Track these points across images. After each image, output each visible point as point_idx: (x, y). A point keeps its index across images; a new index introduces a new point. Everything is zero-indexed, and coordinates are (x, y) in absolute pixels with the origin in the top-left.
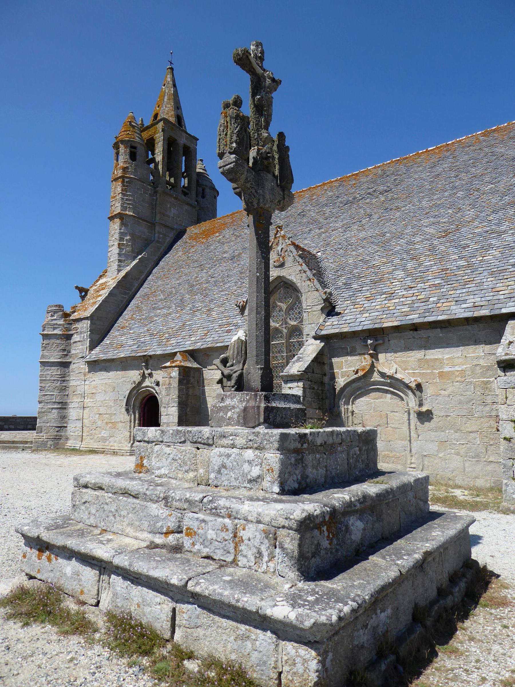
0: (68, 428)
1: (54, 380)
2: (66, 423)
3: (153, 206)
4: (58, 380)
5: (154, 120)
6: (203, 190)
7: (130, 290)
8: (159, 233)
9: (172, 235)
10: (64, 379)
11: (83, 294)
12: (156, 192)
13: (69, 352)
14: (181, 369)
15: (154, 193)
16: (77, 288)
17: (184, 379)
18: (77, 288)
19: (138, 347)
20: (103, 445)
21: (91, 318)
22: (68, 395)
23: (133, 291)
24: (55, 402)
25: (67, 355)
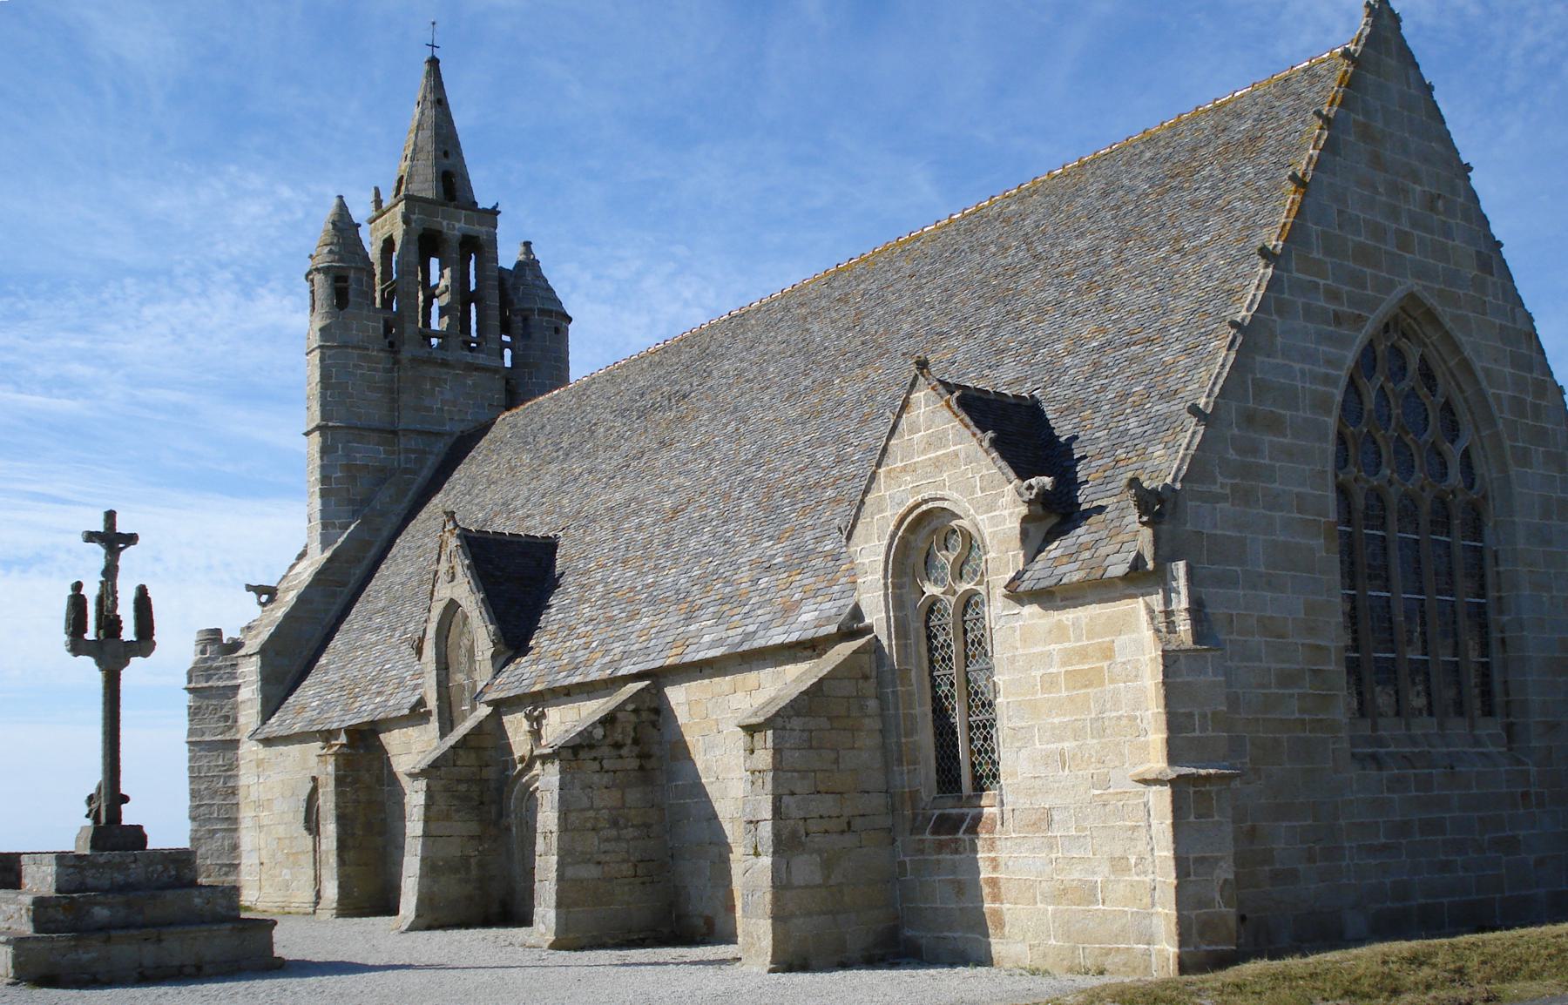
0: (242, 867)
1: (213, 776)
2: (235, 858)
3: (392, 394)
4: (219, 776)
5: (395, 196)
6: (525, 319)
7: (345, 585)
8: (407, 451)
9: (441, 447)
10: (229, 773)
11: (264, 598)
12: (396, 362)
13: (236, 721)
14: (340, 759)
15: (394, 364)
16: (249, 588)
17: (345, 776)
18: (249, 588)
19: (319, 713)
20: (284, 896)
21: (263, 651)
22: (238, 804)
23: (350, 586)
24: (217, 819)
25: (230, 728)
